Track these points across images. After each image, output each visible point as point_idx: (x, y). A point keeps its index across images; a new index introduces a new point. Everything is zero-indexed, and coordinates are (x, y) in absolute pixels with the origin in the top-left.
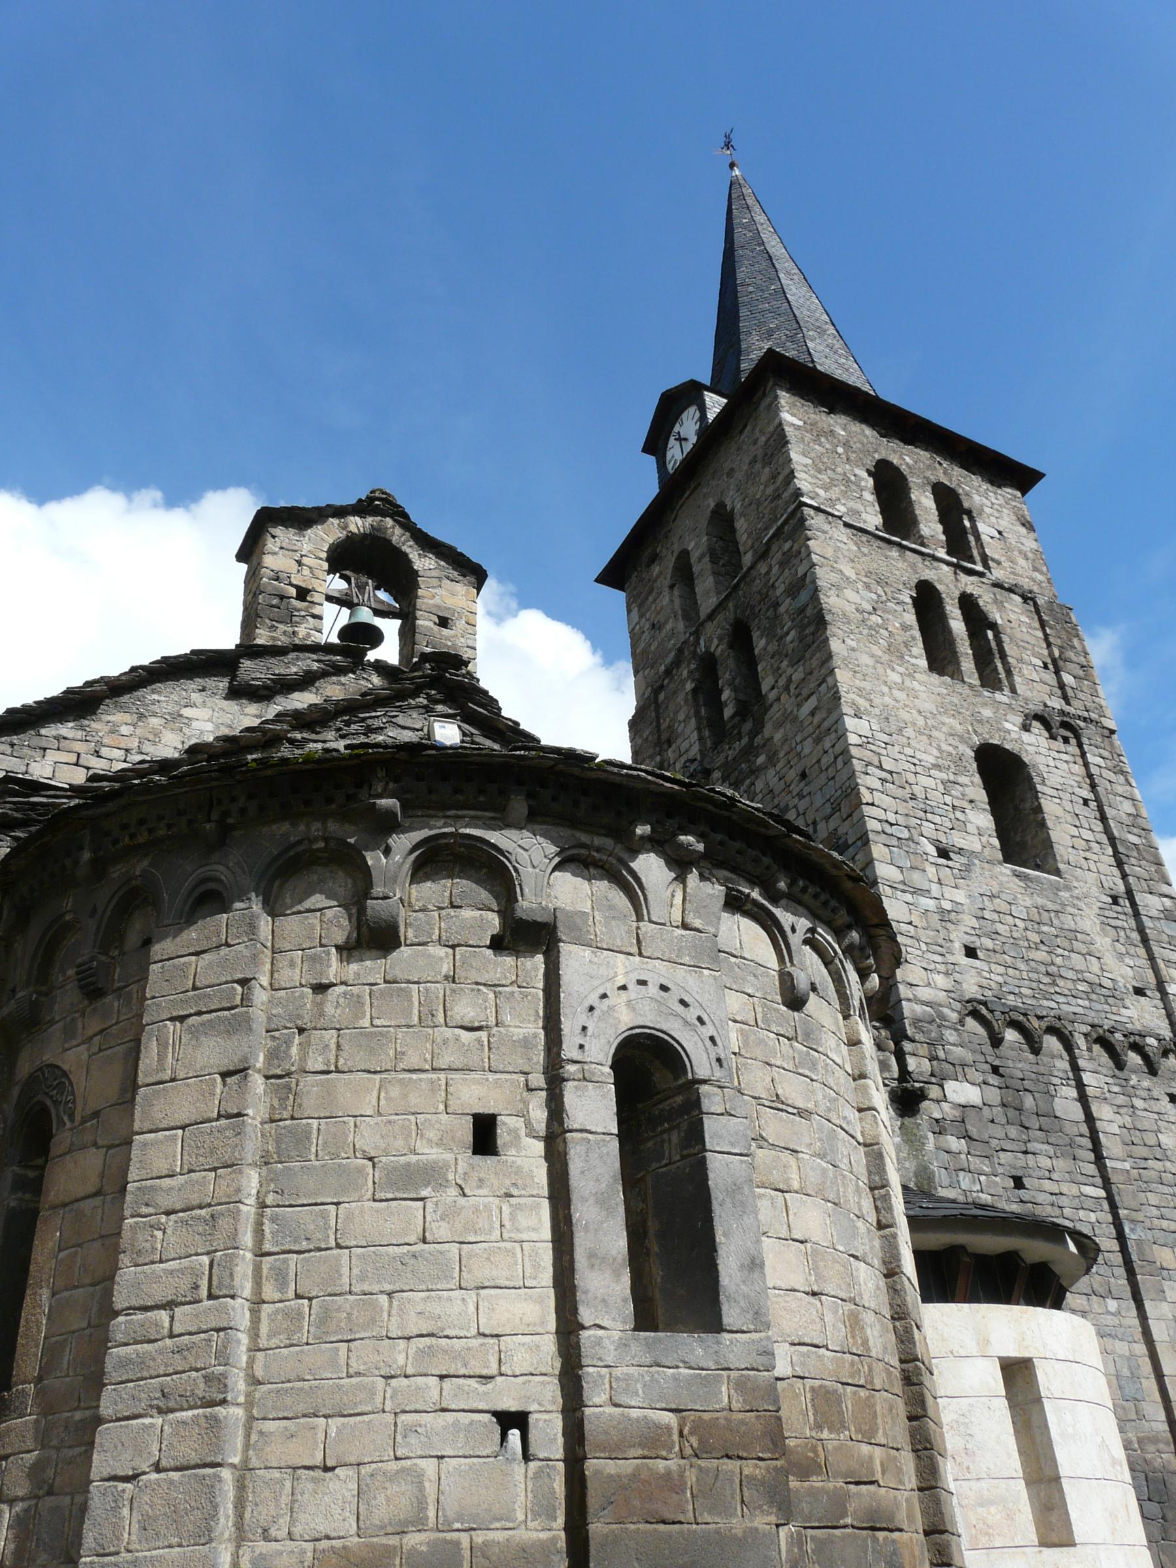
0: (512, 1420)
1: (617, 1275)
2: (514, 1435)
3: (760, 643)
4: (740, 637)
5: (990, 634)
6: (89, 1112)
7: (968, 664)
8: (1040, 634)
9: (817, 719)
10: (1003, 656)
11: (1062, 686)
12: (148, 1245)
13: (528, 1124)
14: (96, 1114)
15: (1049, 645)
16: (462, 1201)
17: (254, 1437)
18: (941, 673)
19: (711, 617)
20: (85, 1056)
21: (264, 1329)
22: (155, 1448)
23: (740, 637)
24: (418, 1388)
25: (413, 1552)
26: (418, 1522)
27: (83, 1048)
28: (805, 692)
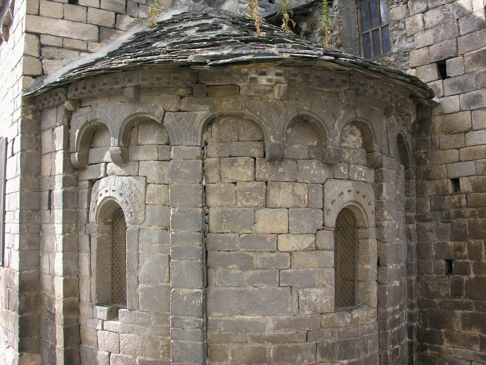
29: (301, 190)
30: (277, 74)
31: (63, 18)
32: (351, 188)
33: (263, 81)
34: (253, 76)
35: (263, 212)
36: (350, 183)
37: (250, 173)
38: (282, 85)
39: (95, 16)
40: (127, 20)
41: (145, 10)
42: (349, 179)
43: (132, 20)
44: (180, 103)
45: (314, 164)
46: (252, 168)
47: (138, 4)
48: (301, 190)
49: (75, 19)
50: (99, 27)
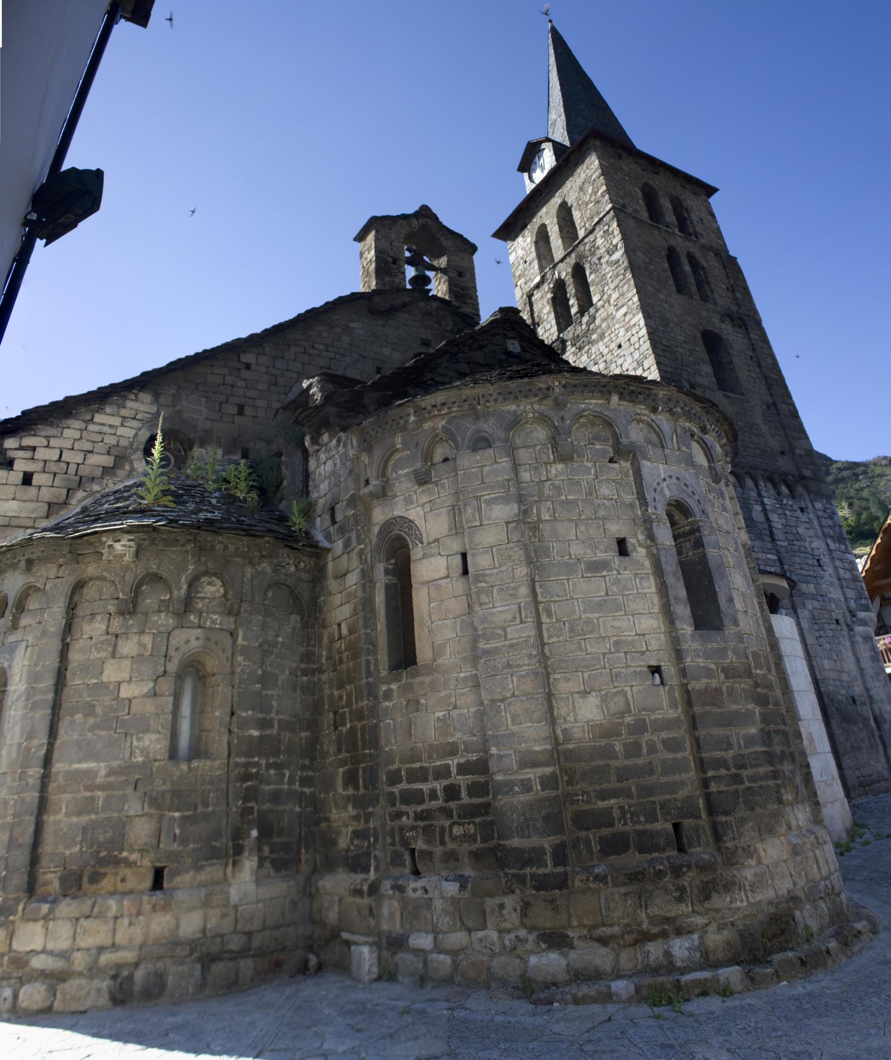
0: (656, 670)
1: (686, 607)
2: (657, 675)
3: (590, 278)
4: (579, 272)
5: (702, 273)
6: (431, 539)
7: (694, 288)
8: (723, 272)
9: (627, 319)
10: (708, 283)
11: (736, 299)
12: (487, 601)
13: (638, 541)
14: (437, 540)
15: (728, 278)
16: (619, 576)
17: (551, 681)
18: (683, 294)
19: (562, 261)
20: (422, 513)
21: (545, 635)
22: (511, 686)
23: (579, 272)
24: (618, 658)
25: (628, 724)
26: (629, 711)
27: (419, 509)
28: (620, 304)
29: (147, 639)
30: (129, 540)
31: (14, 499)
32: (201, 636)
33: (118, 546)
34: (110, 543)
35: (111, 661)
36: (199, 630)
37: (104, 627)
38: (132, 549)
39: (46, 494)
40: (80, 494)
41: (99, 484)
42: (200, 627)
43: (85, 494)
44: (58, 571)
45: (163, 615)
46: (106, 623)
47: (93, 479)
48: (147, 639)
49: (26, 499)
50: (49, 504)
